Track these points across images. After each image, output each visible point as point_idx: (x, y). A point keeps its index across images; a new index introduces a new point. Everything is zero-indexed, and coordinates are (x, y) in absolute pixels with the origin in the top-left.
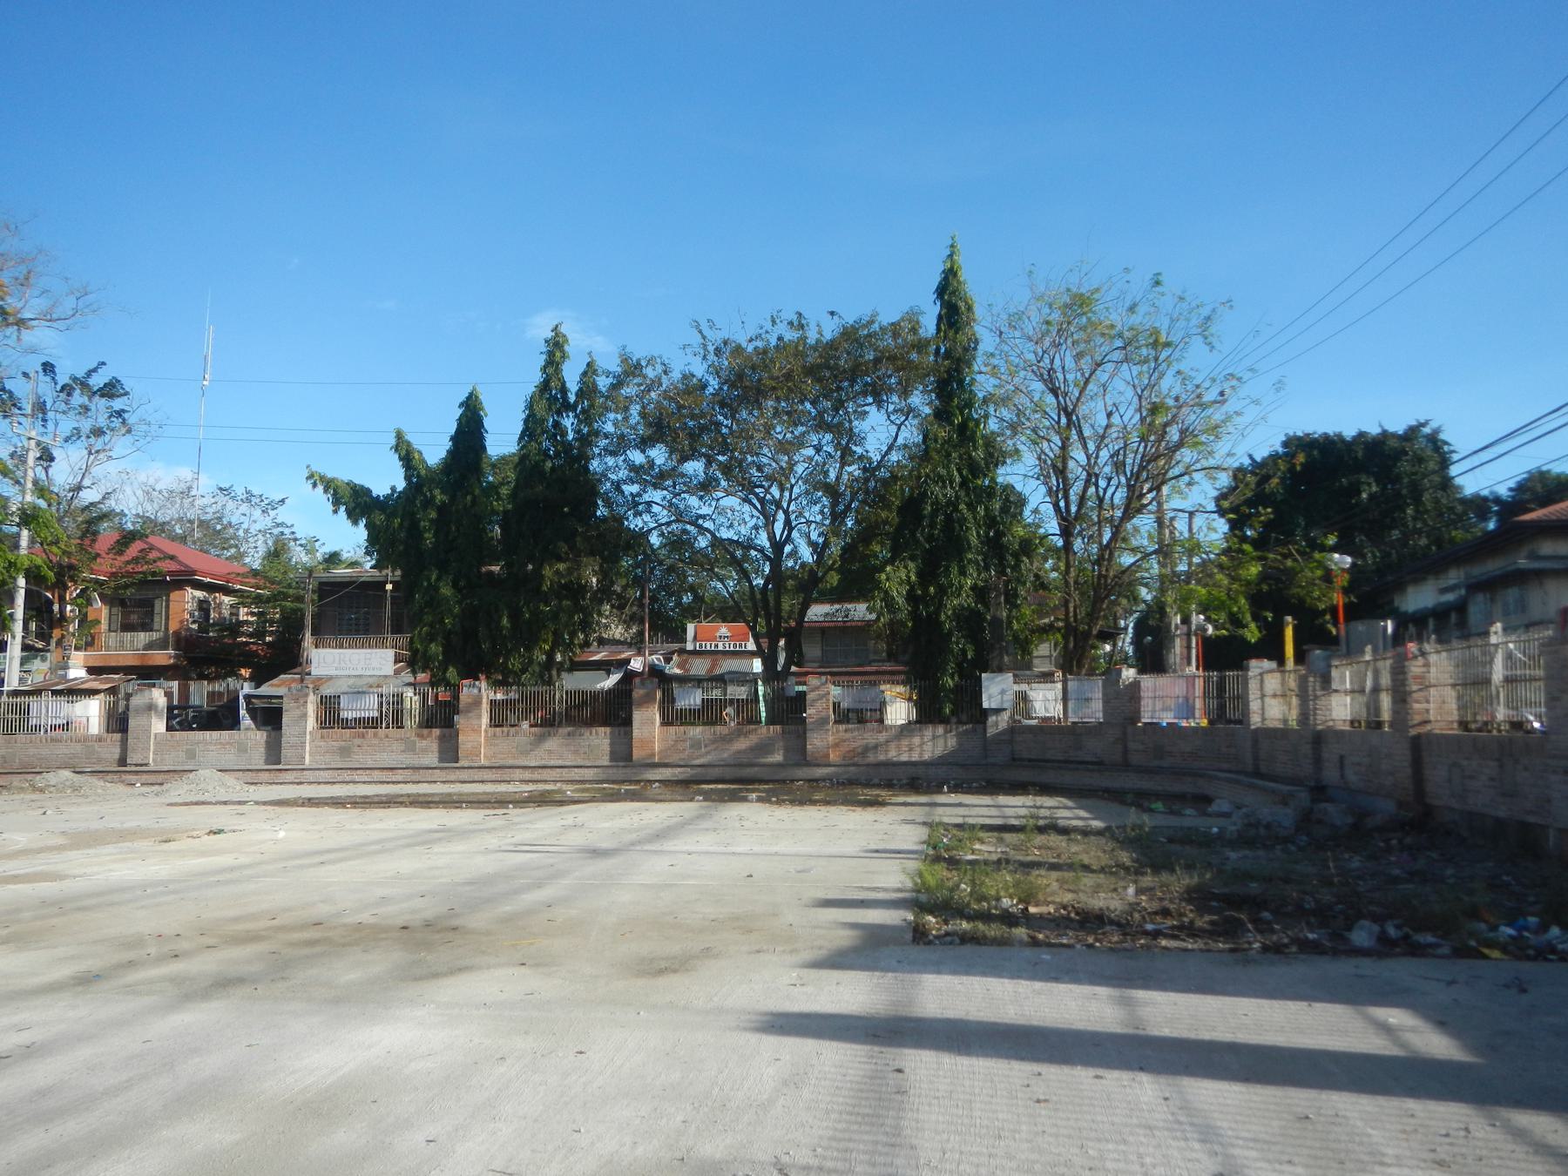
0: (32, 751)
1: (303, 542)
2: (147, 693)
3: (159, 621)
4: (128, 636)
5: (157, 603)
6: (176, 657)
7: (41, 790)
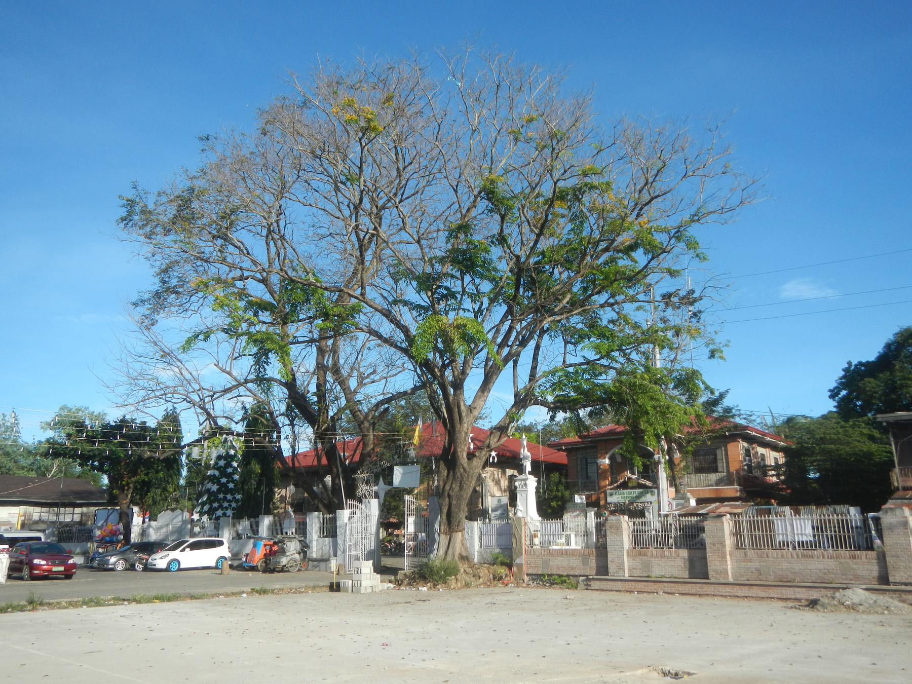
0: (785, 565)
1: (745, 416)
2: (898, 512)
3: (721, 465)
4: (702, 476)
5: (718, 452)
6: (741, 491)
7: (853, 608)
